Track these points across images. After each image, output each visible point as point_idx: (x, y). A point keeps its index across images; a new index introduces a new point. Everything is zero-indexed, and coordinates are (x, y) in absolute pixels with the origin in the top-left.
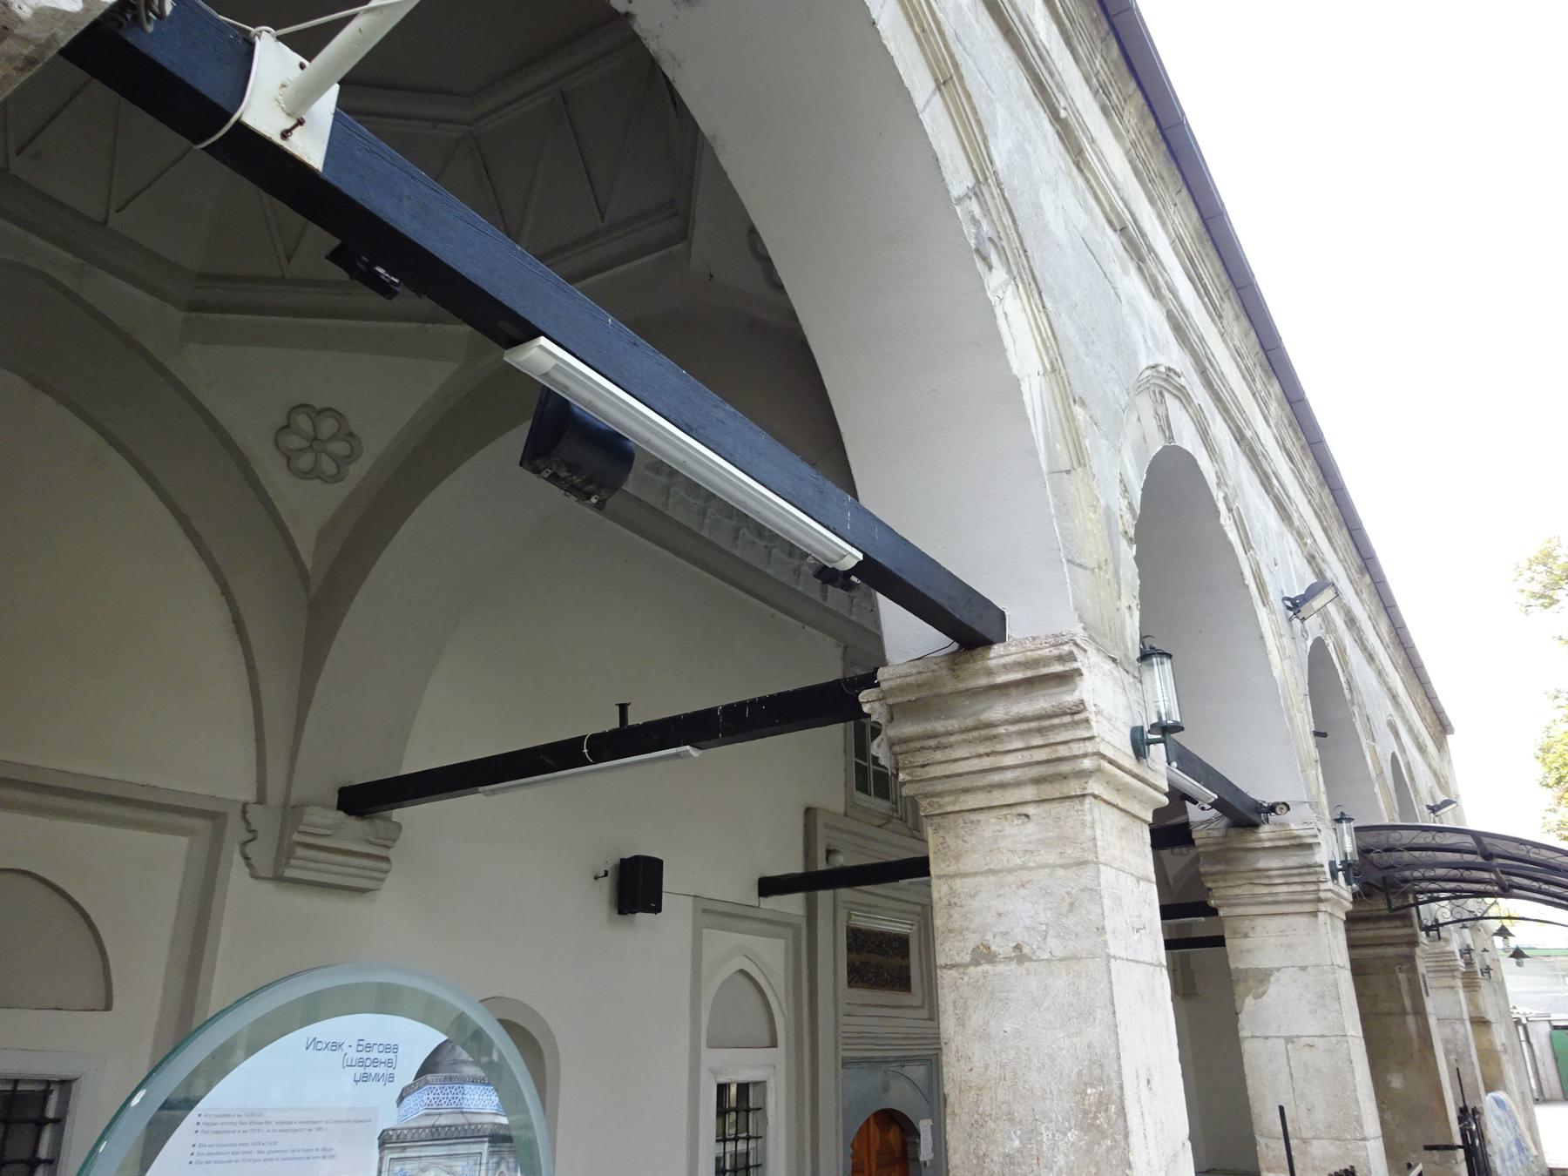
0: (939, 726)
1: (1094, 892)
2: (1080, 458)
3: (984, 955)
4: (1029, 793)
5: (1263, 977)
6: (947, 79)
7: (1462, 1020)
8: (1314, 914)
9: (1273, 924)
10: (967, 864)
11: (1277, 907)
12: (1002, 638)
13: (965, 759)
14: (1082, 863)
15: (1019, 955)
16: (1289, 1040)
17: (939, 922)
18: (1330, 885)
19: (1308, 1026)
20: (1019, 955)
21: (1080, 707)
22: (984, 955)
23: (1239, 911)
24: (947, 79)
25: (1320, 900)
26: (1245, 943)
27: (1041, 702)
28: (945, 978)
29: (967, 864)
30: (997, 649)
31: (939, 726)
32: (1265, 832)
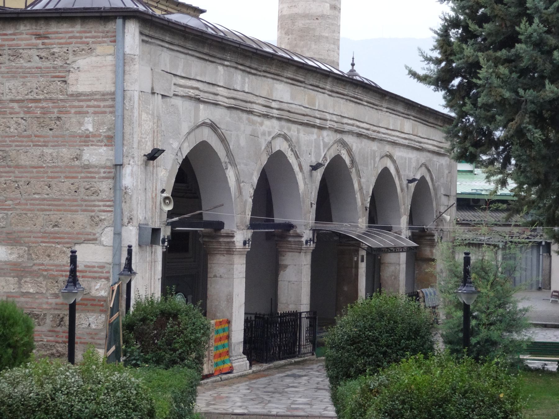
0: (212, 240)
1: (233, 269)
2: (240, 192)
3: (215, 276)
4: (225, 252)
5: (286, 266)
6: (223, 140)
7: (399, 264)
8: (300, 252)
9: (290, 254)
10: (214, 262)
11: (292, 250)
12: (223, 228)
13: (215, 246)
14: (231, 264)
15: (221, 277)
16: (289, 282)
17: (209, 270)
18: (305, 246)
19: (293, 279)
20: (221, 277)
21: (234, 242)
22: (215, 276)
23: (283, 250)
24: (223, 140)
25: (301, 249)
26: (283, 258)
27: (228, 240)
28: (209, 279)
29: (214, 262)
30: (222, 230)
31: (212, 240)
32: (291, 232)
